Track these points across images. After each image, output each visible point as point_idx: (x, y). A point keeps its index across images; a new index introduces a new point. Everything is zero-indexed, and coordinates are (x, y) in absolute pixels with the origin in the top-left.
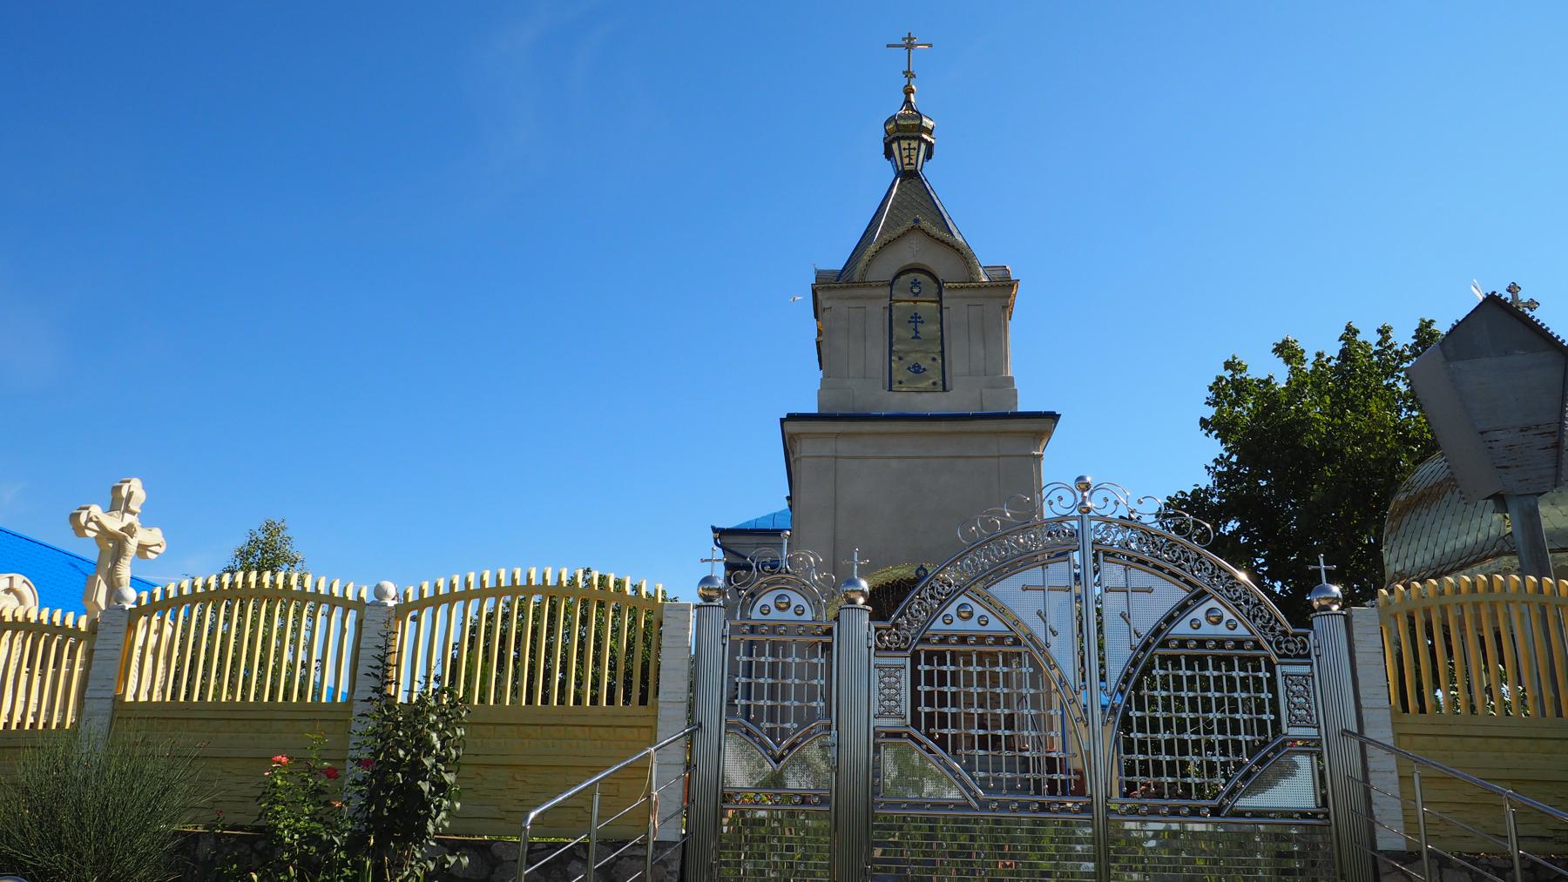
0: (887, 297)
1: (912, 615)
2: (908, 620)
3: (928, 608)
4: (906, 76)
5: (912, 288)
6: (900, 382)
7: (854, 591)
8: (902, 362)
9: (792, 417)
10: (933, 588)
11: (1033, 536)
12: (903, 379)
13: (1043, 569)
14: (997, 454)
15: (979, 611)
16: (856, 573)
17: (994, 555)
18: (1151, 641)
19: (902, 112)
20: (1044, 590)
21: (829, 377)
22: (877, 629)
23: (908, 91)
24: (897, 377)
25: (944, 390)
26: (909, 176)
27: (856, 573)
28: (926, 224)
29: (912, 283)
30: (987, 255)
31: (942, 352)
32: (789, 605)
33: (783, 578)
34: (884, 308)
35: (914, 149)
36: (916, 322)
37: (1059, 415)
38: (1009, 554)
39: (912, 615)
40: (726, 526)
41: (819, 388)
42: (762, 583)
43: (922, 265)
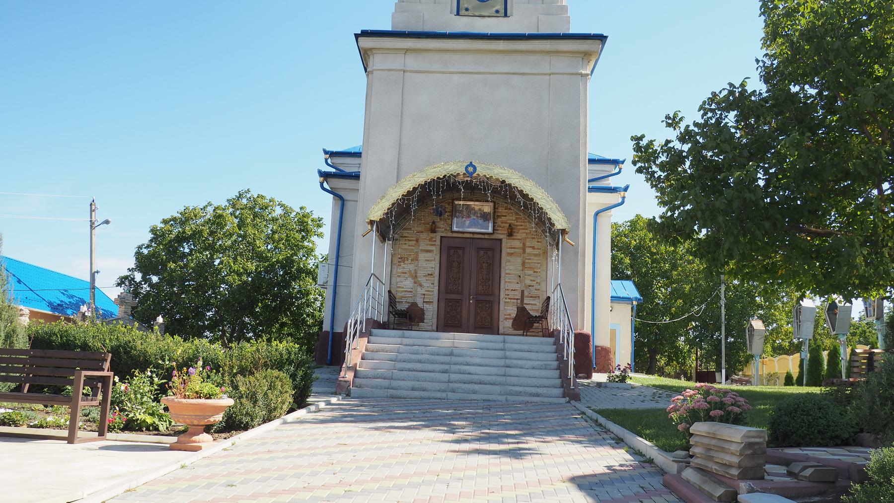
9: (365, 34)
12: (470, 7)
14: (548, 72)
25: (506, 15)
37: (606, 37)
40: (335, 150)
41: (394, 11)
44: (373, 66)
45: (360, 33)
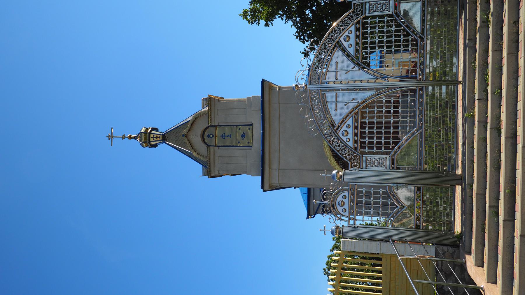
0: (214, 149)
1: (346, 154)
2: (348, 155)
3: (343, 147)
4: (124, 138)
5: (210, 138)
6: (249, 143)
7: (337, 176)
8: (240, 142)
9: (263, 187)
10: (336, 145)
11: (316, 107)
12: (248, 141)
13: (328, 103)
14: (278, 105)
15: (344, 128)
16: (329, 175)
17: (323, 122)
18: (356, 63)
19: (139, 140)
20: (336, 103)
21: (246, 171)
22: (352, 167)
23: (130, 138)
24: (246, 144)
25: (252, 125)
26: (165, 138)
27: (329, 175)
28: (185, 132)
29: (208, 137)
30: (197, 107)
31: (237, 126)
32: (342, 201)
33: (332, 203)
34: (218, 149)
35: (154, 135)
36: (224, 136)
37: (263, 79)
38: (323, 116)
39: (346, 154)
40: (306, 213)
42: (334, 211)
43: (201, 133)
44: (277, 183)
45: (262, 190)
